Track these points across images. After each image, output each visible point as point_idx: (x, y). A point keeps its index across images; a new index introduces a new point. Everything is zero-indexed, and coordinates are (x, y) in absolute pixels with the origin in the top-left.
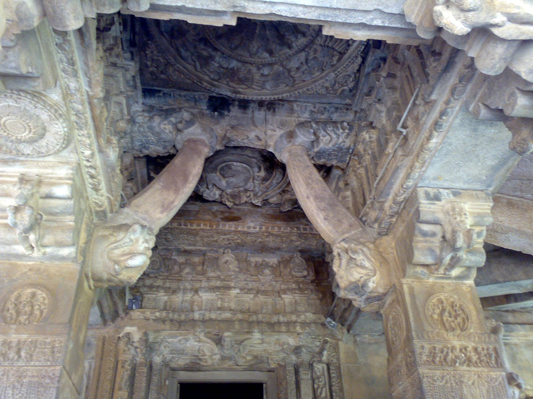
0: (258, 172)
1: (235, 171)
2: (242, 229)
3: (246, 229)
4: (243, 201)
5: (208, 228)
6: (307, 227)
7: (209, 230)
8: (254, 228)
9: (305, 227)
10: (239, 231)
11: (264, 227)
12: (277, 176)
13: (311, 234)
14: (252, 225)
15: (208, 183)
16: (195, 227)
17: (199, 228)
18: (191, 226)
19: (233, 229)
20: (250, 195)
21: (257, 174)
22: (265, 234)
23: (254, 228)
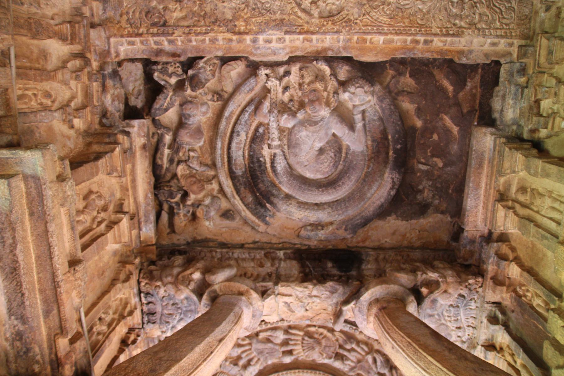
0: (275, 155)
1: (317, 171)
2: (296, 36)
3: (287, 37)
4: (295, 69)
5: (369, 37)
6: (155, 47)
7: (369, 33)
8: (269, 42)
9: (159, 47)
10: (300, 33)
11: (248, 42)
12: (241, 153)
13: (140, 35)
14: (274, 45)
15: (362, 134)
16: (396, 38)
17: (389, 37)
18: (405, 41)
19: (314, 37)
20: (283, 93)
21: (278, 151)
22: (241, 25)
23: (269, 42)
